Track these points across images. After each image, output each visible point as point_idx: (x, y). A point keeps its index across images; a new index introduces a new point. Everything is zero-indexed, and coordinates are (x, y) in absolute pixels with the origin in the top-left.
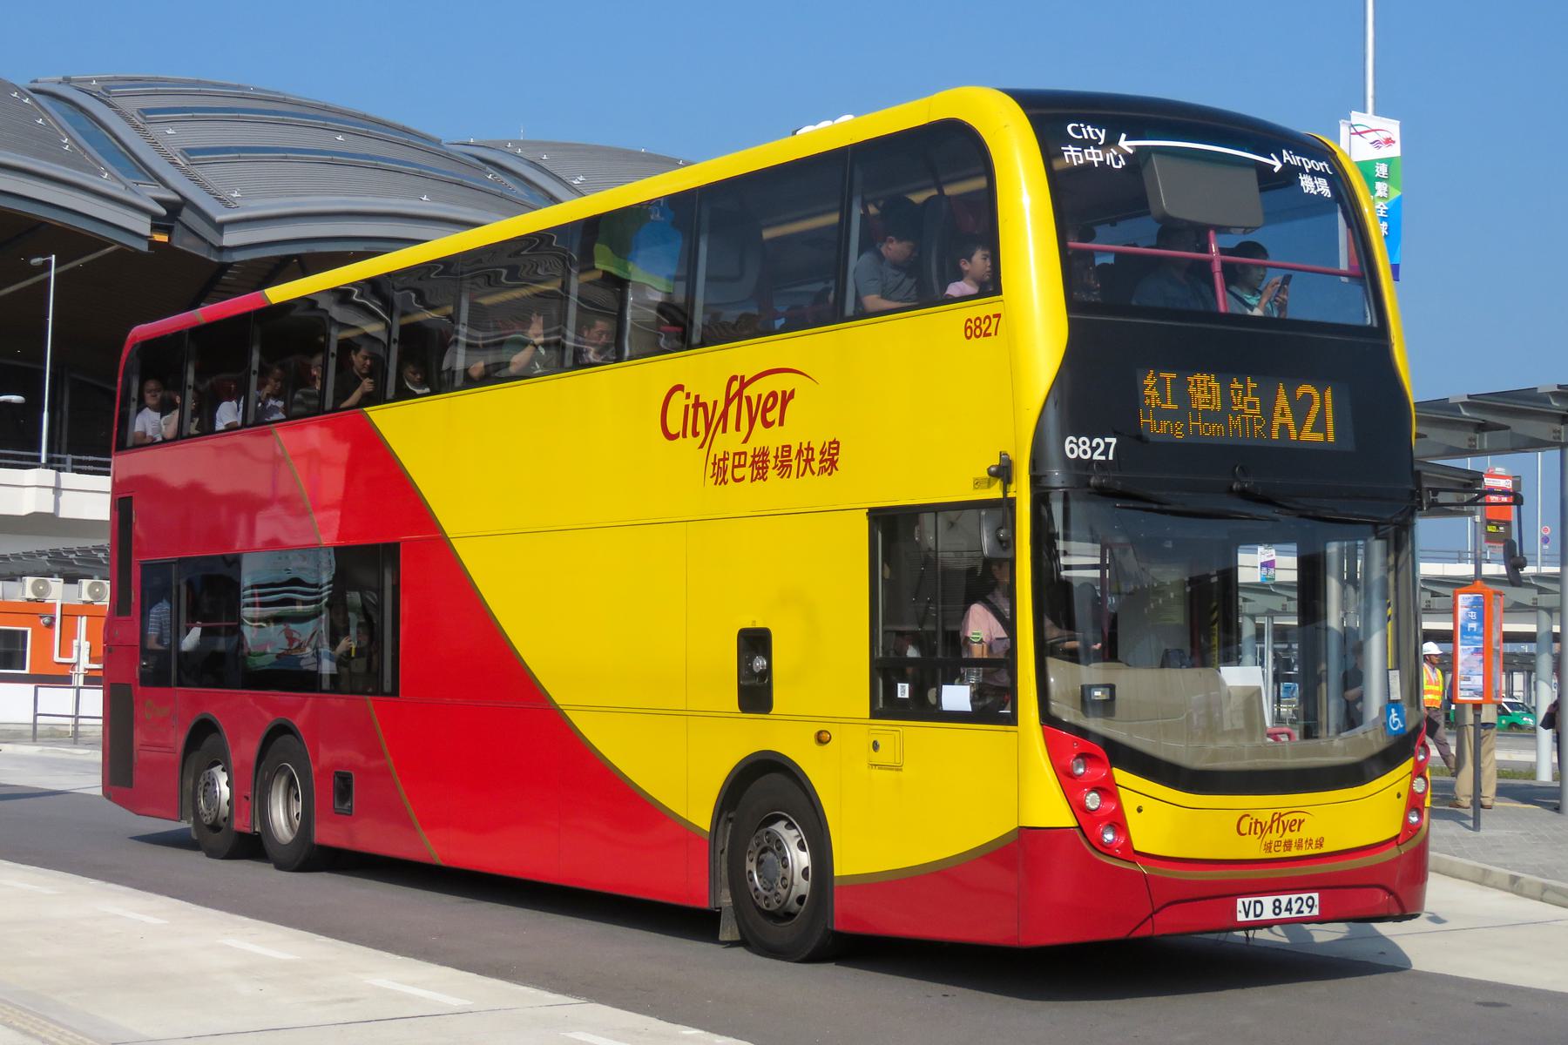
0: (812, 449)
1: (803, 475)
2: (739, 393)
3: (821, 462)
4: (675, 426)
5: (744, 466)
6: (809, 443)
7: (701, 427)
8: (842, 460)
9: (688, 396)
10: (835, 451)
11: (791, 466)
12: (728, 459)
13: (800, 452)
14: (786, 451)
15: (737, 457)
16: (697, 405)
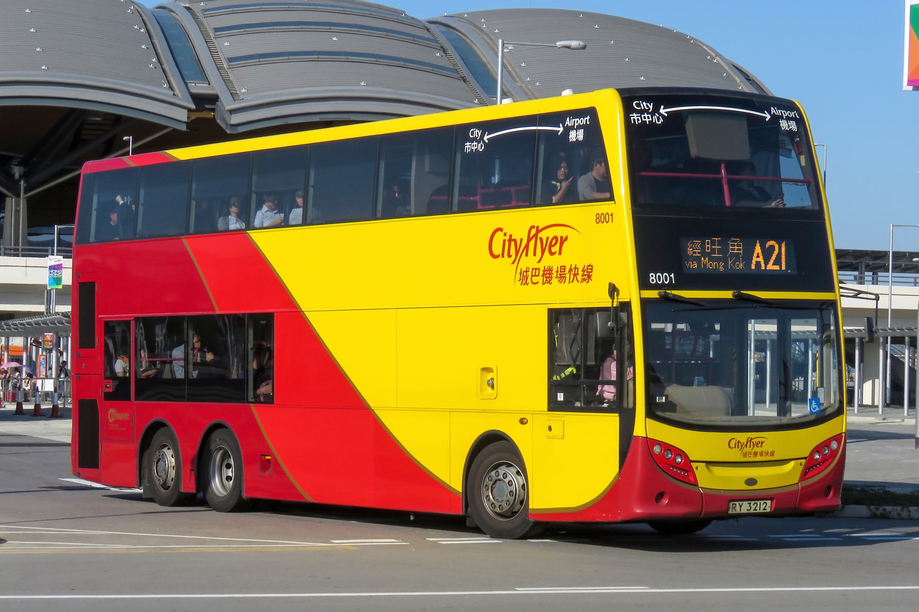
0: (578, 269)
1: (572, 282)
2: (536, 235)
3: (583, 275)
4: (497, 250)
5: (538, 276)
6: (576, 265)
7: (513, 252)
8: (594, 275)
9: (505, 234)
10: (589, 270)
11: (565, 277)
12: (529, 271)
13: (570, 270)
14: (563, 269)
15: (534, 271)
16: (510, 240)
